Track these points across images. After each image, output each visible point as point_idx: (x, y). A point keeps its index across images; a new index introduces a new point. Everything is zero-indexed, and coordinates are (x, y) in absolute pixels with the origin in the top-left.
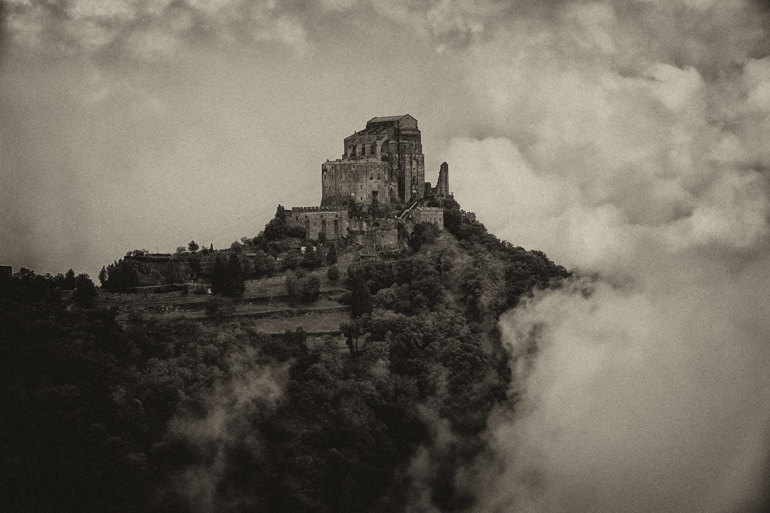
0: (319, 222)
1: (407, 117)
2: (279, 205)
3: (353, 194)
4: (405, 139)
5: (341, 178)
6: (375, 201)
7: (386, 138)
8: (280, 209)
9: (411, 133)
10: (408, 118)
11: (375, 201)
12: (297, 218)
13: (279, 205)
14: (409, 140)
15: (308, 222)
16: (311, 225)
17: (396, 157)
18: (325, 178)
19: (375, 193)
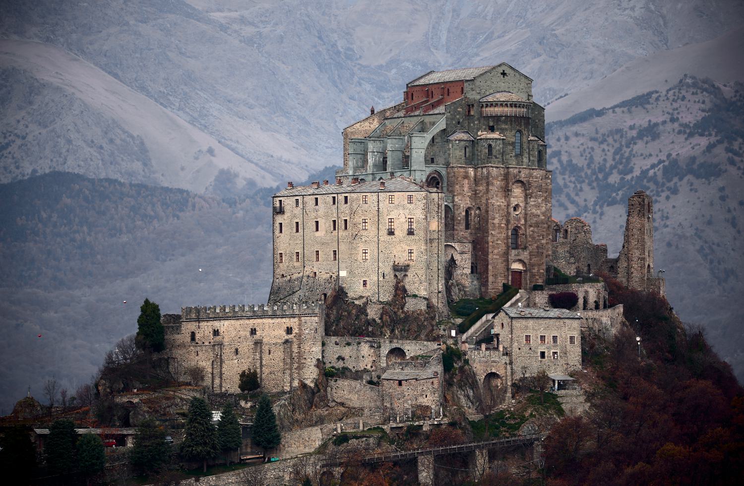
0: (246, 347)
1: (501, 70)
2: (147, 302)
3: (343, 274)
4: (492, 129)
5: (317, 230)
6: (400, 292)
7: (441, 124)
8: (150, 312)
9: (508, 111)
10: (504, 74)
11: (400, 292)
12: (193, 335)
13: (147, 302)
14: (502, 131)
15: (221, 344)
16: (228, 352)
17: (466, 177)
18: (281, 232)
19: (400, 270)
